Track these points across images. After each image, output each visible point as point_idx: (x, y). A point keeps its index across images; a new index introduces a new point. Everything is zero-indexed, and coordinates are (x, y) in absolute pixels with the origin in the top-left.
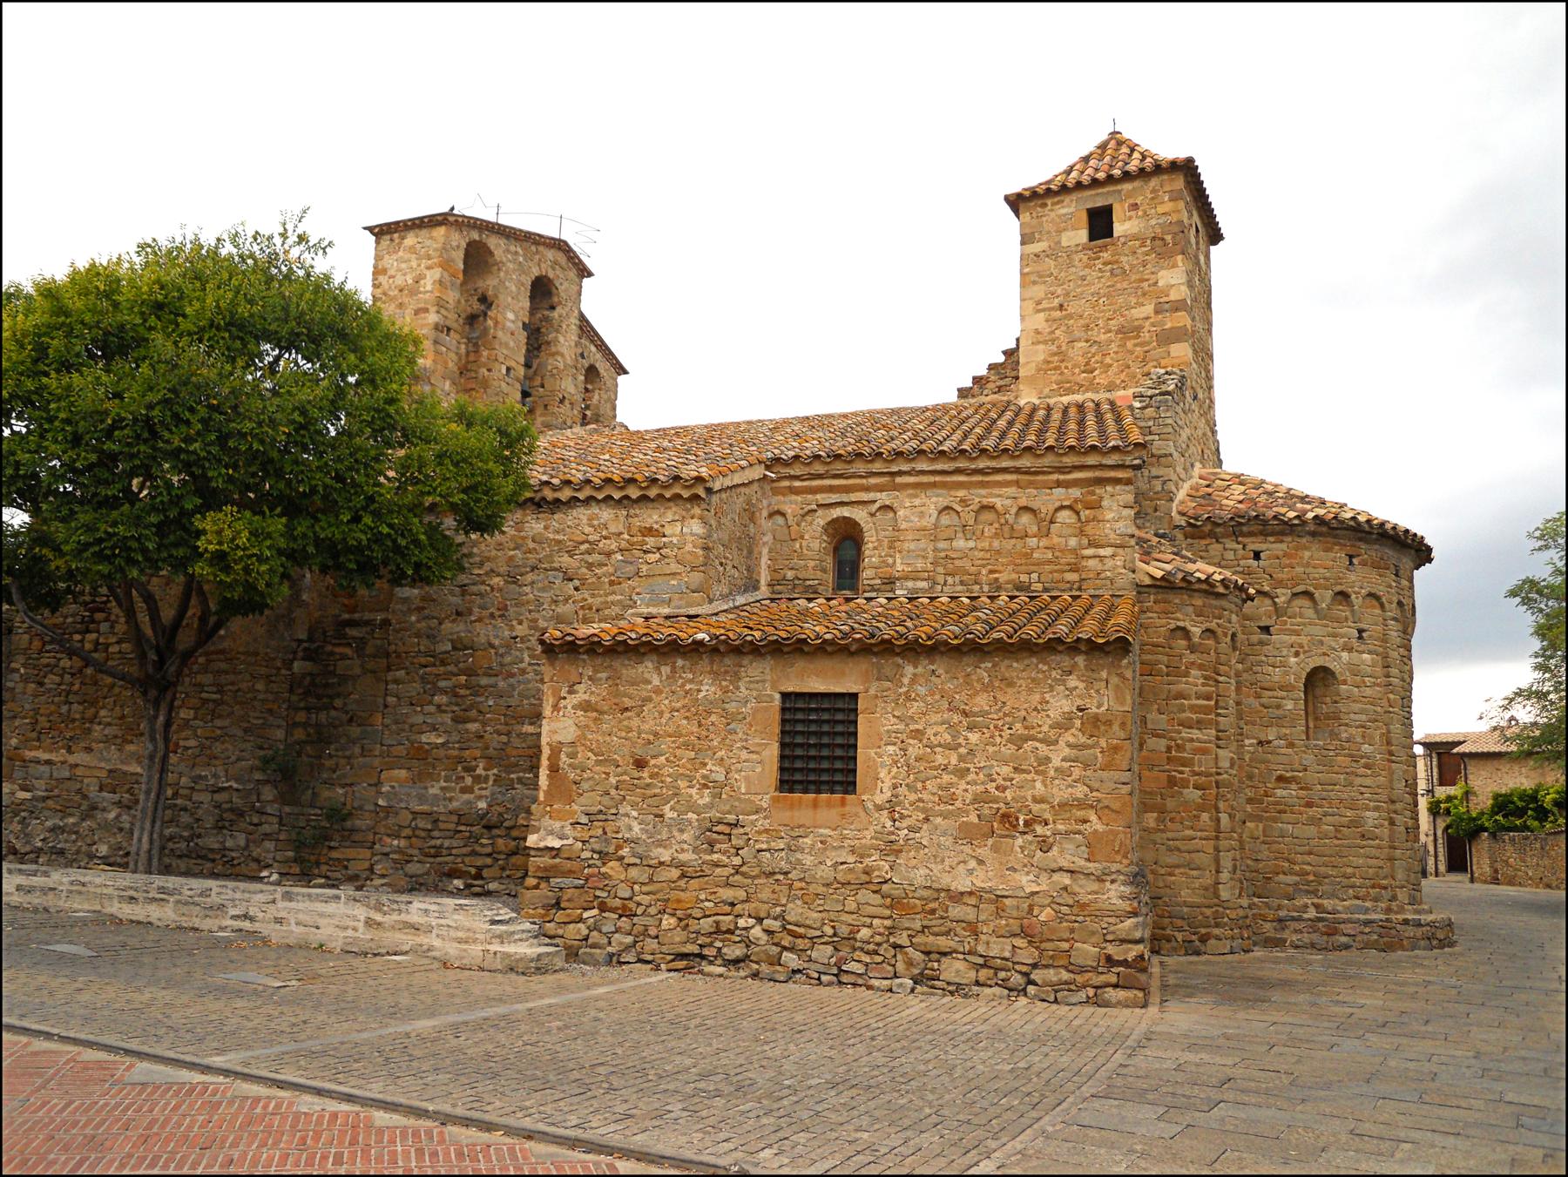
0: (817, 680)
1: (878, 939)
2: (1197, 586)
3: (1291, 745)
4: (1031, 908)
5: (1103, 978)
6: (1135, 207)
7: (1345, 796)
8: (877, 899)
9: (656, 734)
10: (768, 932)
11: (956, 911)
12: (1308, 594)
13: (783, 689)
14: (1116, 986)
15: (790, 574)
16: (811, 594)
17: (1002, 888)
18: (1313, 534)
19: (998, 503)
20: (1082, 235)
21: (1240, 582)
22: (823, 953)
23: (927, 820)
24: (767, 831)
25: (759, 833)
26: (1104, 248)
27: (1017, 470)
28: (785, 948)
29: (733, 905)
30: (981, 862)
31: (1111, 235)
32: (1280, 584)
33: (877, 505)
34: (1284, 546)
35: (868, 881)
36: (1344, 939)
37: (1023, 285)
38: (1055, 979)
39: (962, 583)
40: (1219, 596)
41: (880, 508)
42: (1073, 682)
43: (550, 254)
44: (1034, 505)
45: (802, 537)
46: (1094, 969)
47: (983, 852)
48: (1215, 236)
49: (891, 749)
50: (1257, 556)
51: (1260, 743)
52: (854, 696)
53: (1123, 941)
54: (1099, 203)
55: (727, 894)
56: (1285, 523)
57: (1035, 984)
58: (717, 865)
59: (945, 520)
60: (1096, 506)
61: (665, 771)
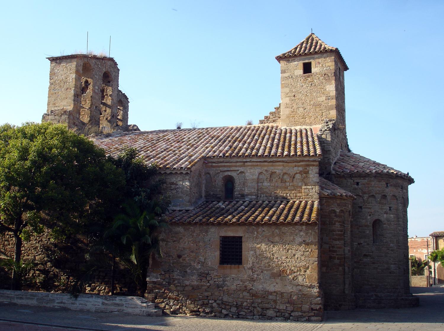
0: (231, 233)
1: (249, 305)
2: (338, 197)
3: (368, 244)
4: (291, 295)
5: (310, 314)
6: (319, 63)
8: (248, 295)
9: (184, 248)
10: (218, 304)
11: (270, 297)
12: (373, 196)
13: (221, 235)
14: (313, 316)
15: (212, 193)
16: (219, 200)
17: (283, 291)
18: (375, 177)
19: (277, 171)
20: (301, 72)
21: (351, 195)
22: (234, 310)
23: (262, 272)
24: (217, 276)
25: (215, 276)
26: (308, 77)
27: (283, 162)
28: (223, 308)
29: (208, 297)
30: (277, 283)
31: (311, 72)
32: (364, 193)
33: (239, 171)
34: (366, 181)
35: (246, 289)
37: (282, 88)
38: (297, 315)
39: (266, 196)
40: (344, 199)
41: (240, 172)
42: (302, 233)
43: (109, 63)
44: (289, 172)
45: (215, 181)
46: (308, 312)
47: (278, 281)
48: (346, 68)
49: (252, 252)
50: (358, 184)
51: (359, 244)
52: (241, 237)
53: (315, 304)
54: (307, 61)
55: (206, 294)
56: (367, 174)
57: (292, 316)
58: (202, 286)
59: (261, 177)
60: (307, 173)
61: (187, 259)
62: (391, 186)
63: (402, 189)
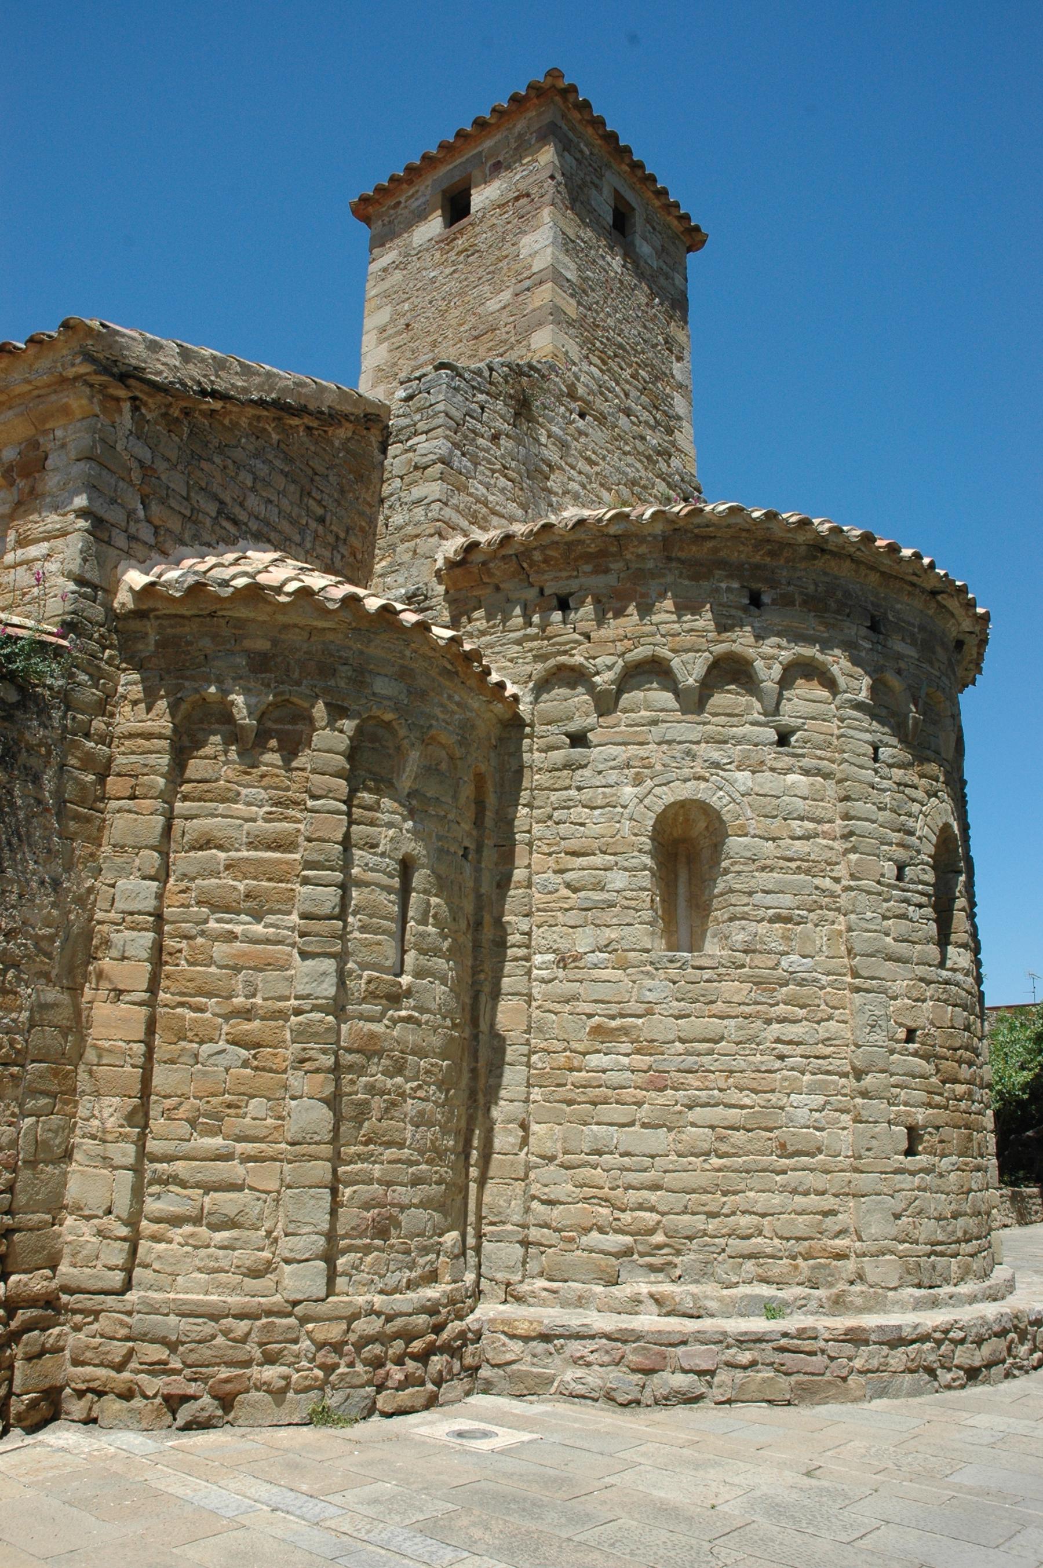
7: (740, 1063)
36: (680, 1381)
62: (785, 601)
63: (874, 627)
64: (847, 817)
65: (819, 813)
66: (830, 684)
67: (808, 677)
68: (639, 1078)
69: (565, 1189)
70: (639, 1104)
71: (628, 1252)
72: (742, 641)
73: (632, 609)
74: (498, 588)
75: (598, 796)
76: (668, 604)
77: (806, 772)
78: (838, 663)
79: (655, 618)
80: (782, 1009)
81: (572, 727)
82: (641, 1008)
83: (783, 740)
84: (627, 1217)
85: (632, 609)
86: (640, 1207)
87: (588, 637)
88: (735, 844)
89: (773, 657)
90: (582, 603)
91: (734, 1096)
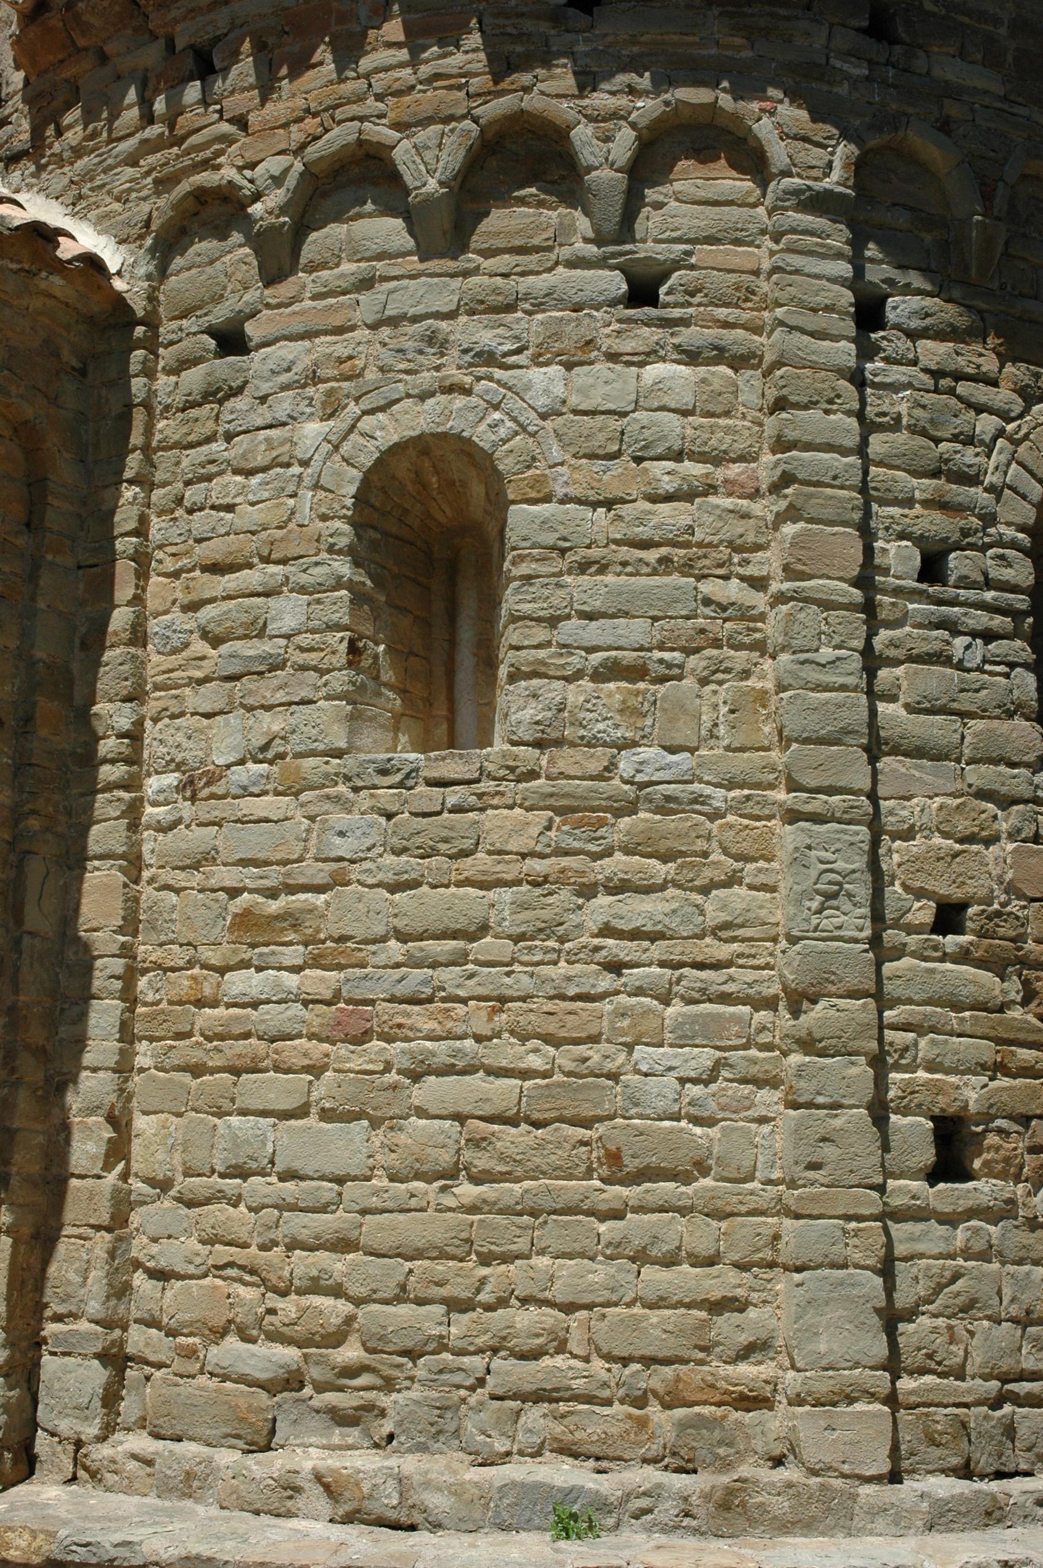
63: (879, 29)
64: (781, 445)
65: (719, 441)
66: (752, 161)
67: (704, 154)
68: (316, 1017)
69: (181, 1251)
70: (316, 1070)
71: (291, 1381)
72: (548, 91)
73: (323, 53)
74: (103, 58)
75: (254, 448)
76: (393, 29)
77: (691, 357)
78: (775, 121)
79: (366, 63)
80: (618, 864)
81: (219, 314)
82: (320, 872)
83: (642, 291)
84: (288, 1307)
85: (323, 53)
86: (315, 1286)
87: (241, 122)
88: (523, 519)
89: (615, 115)
90: (234, 56)
91: (507, 1051)
